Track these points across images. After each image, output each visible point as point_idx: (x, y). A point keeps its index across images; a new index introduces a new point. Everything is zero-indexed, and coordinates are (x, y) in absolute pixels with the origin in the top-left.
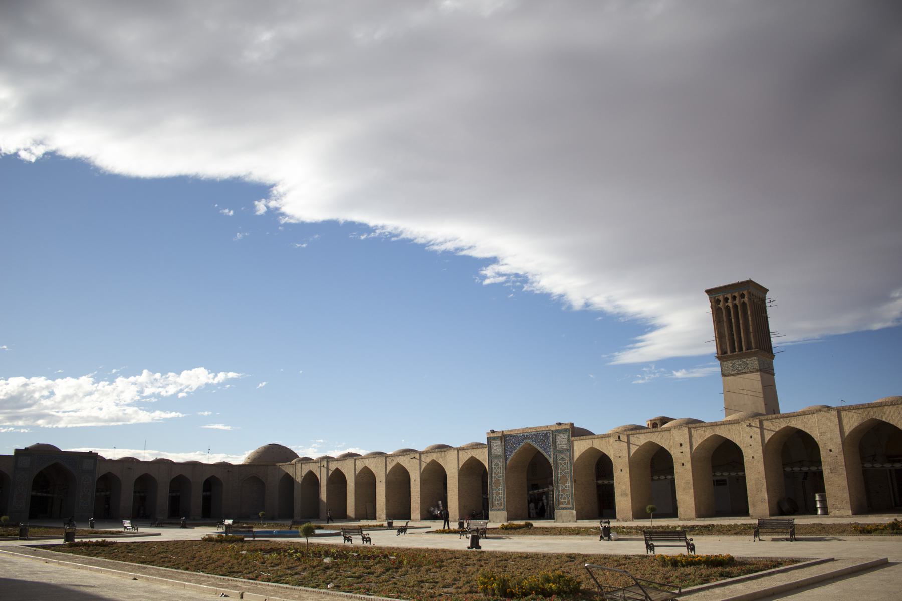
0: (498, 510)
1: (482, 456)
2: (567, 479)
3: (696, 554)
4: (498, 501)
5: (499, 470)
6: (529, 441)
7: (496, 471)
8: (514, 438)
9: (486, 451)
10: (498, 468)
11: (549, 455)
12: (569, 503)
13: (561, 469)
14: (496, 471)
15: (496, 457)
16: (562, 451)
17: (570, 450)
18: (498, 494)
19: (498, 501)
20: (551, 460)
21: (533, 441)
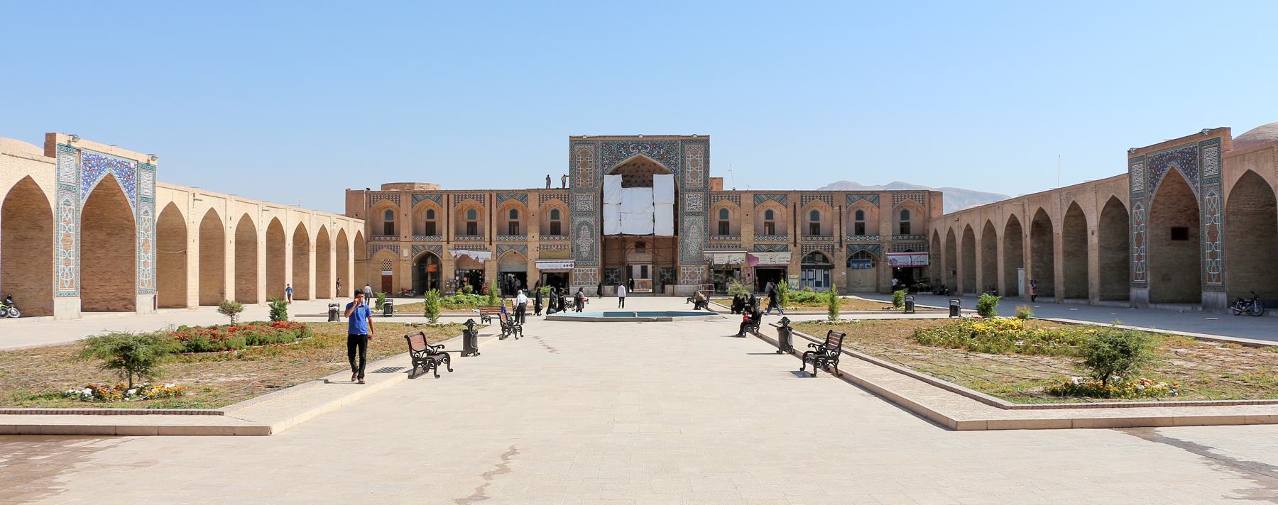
2: (149, 246)
5: (70, 216)
6: (113, 172)
9: (51, 169)
10: (70, 209)
11: (133, 202)
16: (145, 199)
17: (151, 200)
19: (67, 277)
20: (134, 210)
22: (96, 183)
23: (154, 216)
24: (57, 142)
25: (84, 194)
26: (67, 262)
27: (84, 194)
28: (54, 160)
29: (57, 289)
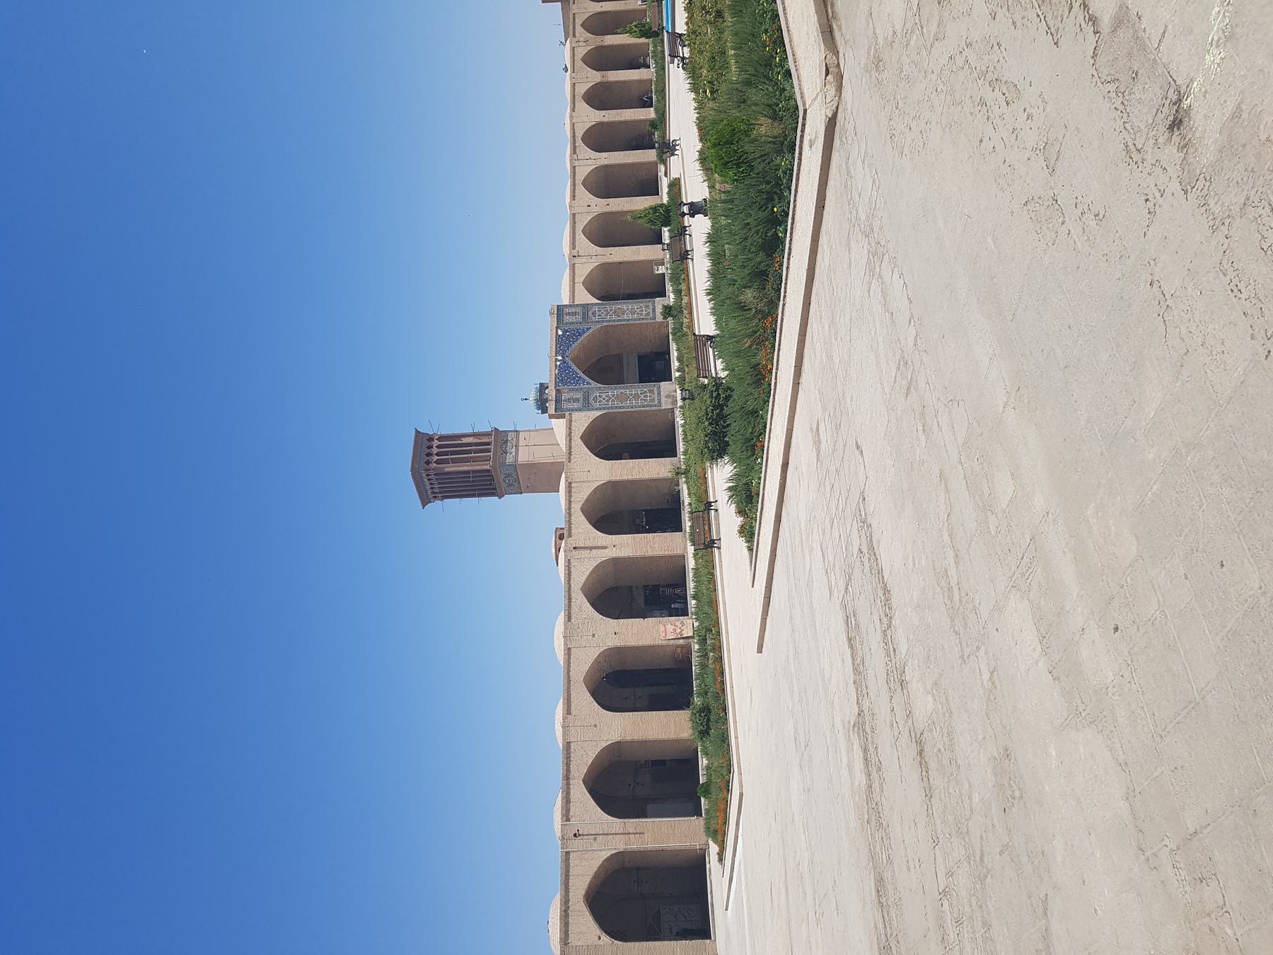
0: (659, 394)
1: (583, 420)
3: (685, 32)
4: (646, 396)
5: (604, 396)
7: (604, 399)
8: (561, 375)
9: (576, 415)
12: (646, 307)
13: (606, 315)
14: (604, 399)
15: (586, 399)
17: (586, 307)
18: (636, 396)
19: (646, 396)
20: (595, 328)
21: (568, 348)
22: (578, 371)
23: (596, 304)
24: (554, 413)
25: (588, 383)
26: (636, 396)
27: (588, 383)
28: (567, 413)
29: (655, 406)
